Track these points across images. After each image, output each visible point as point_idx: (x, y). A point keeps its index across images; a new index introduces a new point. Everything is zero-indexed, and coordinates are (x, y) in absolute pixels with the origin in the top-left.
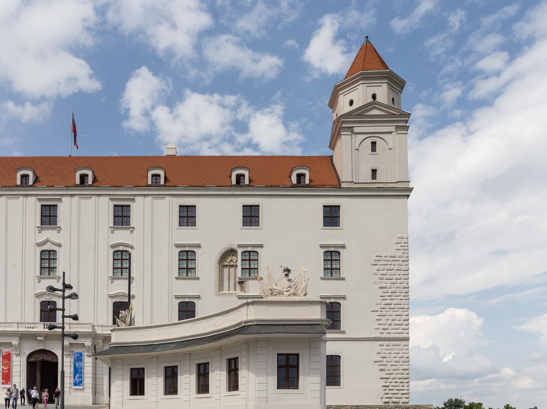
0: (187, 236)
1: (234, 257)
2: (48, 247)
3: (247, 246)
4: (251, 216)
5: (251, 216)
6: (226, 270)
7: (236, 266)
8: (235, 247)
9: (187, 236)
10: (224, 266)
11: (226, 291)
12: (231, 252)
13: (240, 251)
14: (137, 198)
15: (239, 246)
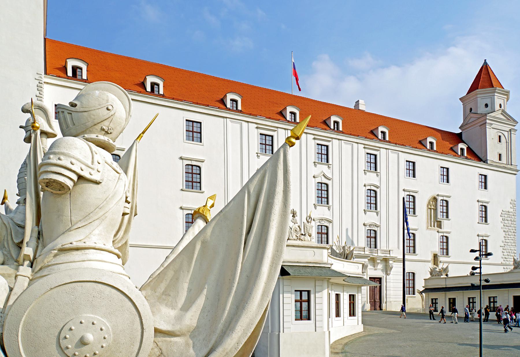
9: (410, 184)
12: (435, 199)
15: (438, 195)
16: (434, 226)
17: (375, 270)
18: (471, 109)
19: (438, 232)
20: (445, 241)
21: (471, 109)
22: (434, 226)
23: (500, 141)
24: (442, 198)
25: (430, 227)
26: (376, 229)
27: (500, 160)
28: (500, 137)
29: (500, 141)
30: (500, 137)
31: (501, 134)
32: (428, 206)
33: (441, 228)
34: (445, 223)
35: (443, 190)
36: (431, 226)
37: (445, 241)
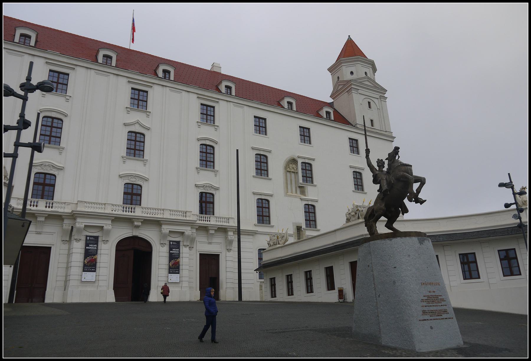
0: (262, 142)
1: (294, 166)
2: (137, 129)
3: (304, 158)
4: (305, 135)
5: (305, 135)
6: (288, 174)
7: (297, 173)
8: (296, 158)
9: (262, 142)
10: (288, 171)
11: (290, 193)
12: (294, 161)
13: (300, 161)
14: (220, 102)
15: (299, 157)
16: (296, 193)
17: (210, 243)
18: (338, 78)
19: (301, 199)
20: (310, 211)
21: (338, 78)
22: (296, 193)
23: (370, 107)
24: (304, 161)
25: (290, 193)
26: (213, 192)
27: (372, 125)
28: (369, 103)
29: (370, 107)
30: (369, 103)
31: (370, 101)
32: (286, 168)
33: (305, 195)
34: (309, 189)
35: (303, 151)
36: (292, 192)
37: (310, 211)
